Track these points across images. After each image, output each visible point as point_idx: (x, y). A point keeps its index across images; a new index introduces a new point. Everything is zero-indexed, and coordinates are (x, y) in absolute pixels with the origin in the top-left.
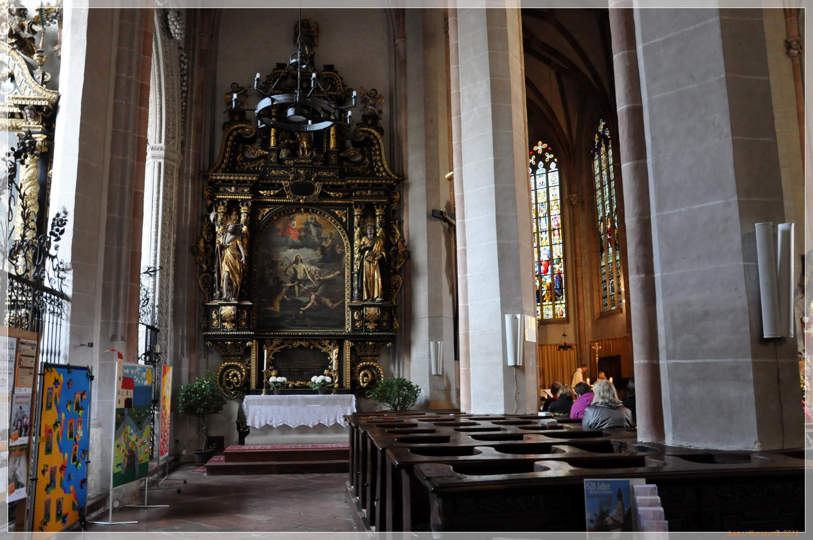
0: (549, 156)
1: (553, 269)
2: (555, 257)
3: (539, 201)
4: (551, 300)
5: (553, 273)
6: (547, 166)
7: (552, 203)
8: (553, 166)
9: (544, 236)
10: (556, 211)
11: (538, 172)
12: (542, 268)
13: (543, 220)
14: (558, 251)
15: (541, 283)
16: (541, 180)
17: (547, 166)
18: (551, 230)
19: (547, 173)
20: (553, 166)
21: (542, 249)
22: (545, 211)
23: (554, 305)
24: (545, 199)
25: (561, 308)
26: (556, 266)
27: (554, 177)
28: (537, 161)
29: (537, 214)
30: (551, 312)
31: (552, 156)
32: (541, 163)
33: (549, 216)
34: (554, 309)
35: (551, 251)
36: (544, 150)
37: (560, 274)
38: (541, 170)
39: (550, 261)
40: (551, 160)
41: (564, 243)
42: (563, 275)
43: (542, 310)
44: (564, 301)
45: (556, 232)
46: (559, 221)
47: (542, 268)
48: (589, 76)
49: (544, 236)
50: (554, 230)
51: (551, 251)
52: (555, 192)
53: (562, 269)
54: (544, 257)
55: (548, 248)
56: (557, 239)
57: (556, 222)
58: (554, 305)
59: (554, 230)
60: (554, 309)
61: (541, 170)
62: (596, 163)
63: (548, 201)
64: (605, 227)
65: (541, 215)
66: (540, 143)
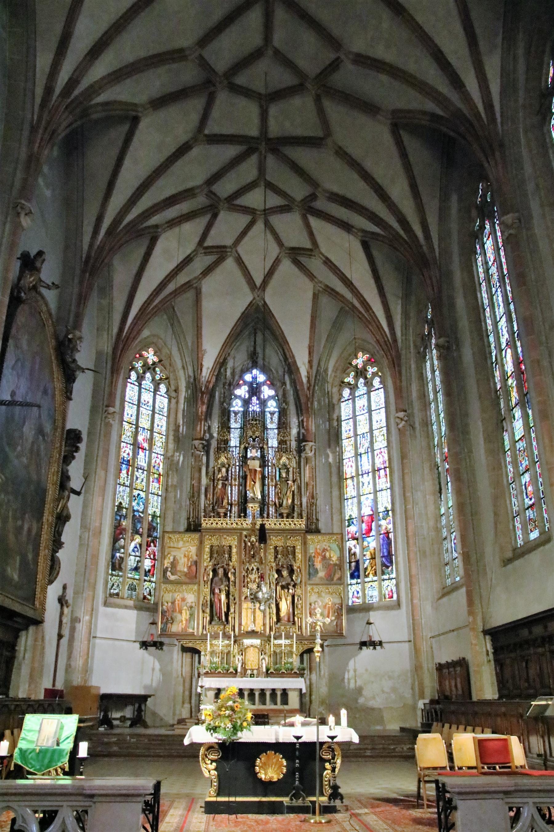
0: (371, 370)
2: (381, 509)
3: (359, 433)
4: (375, 574)
6: (369, 384)
8: (376, 382)
10: (381, 443)
13: (364, 457)
14: (385, 501)
15: (363, 549)
16: (361, 402)
17: (369, 384)
19: (369, 393)
20: (376, 382)
21: (363, 498)
22: (367, 445)
24: (367, 429)
25: (389, 586)
26: (383, 523)
28: (356, 377)
30: (376, 593)
31: (376, 369)
32: (362, 380)
33: (373, 451)
36: (365, 364)
37: (387, 533)
38: (362, 389)
40: (374, 374)
41: (391, 488)
42: (391, 536)
43: (364, 590)
44: (394, 575)
45: (382, 472)
46: (386, 457)
47: (364, 526)
48: (395, 225)
49: (367, 479)
50: (379, 470)
52: (380, 417)
53: (390, 526)
54: (367, 511)
55: (371, 496)
56: (383, 482)
57: (381, 459)
59: (379, 470)
61: (362, 389)
62: (428, 364)
63: (371, 430)
64: (442, 454)
66: (360, 354)
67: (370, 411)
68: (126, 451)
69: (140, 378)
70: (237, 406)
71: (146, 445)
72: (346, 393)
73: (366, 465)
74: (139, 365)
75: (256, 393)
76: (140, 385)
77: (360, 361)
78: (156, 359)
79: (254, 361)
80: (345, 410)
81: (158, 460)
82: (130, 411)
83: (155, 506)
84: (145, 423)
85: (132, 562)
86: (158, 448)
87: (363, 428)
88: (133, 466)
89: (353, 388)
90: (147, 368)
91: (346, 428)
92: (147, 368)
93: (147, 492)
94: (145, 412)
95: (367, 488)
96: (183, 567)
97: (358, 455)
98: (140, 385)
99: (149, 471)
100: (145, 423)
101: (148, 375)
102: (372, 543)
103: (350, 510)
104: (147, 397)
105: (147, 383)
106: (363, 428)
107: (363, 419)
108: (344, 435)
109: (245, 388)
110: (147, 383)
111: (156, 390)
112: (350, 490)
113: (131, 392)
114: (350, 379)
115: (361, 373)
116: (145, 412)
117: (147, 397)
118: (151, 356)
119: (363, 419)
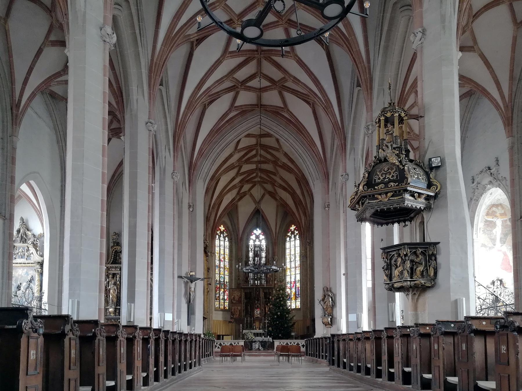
0: (296, 232)
1: (296, 285)
2: (297, 280)
5: (296, 288)
6: (295, 237)
7: (297, 255)
8: (297, 237)
9: (293, 270)
10: (298, 258)
11: (292, 240)
12: (292, 285)
14: (298, 277)
15: (291, 292)
16: (293, 243)
17: (295, 237)
18: (295, 267)
23: (296, 302)
26: (297, 284)
27: (298, 242)
29: (290, 259)
34: (296, 304)
35: (295, 277)
36: (295, 229)
38: (293, 239)
39: (295, 282)
47: (292, 285)
49: (293, 270)
51: (295, 277)
52: (298, 249)
54: (293, 280)
56: (298, 271)
57: (298, 263)
58: (296, 302)
60: (296, 304)
61: (293, 239)
65: (292, 260)
67: (295, 247)
68: (217, 263)
69: (220, 237)
70: (251, 243)
71: (223, 260)
72: (288, 239)
73: (293, 265)
74: (218, 232)
75: (257, 239)
76: (220, 240)
77: (293, 228)
78: (224, 229)
79: (257, 226)
80: (288, 245)
81: (227, 264)
82: (217, 249)
83: (227, 279)
84: (222, 252)
85: (221, 297)
86: (227, 260)
87: (293, 253)
88: (220, 267)
89: (290, 238)
90: (222, 233)
91: (288, 251)
92: (222, 233)
93: (224, 275)
94: (222, 248)
95: (293, 273)
96: (237, 298)
97: (291, 261)
98: (220, 240)
99: (224, 268)
100: (222, 252)
101: (222, 235)
102: (293, 290)
103: (288, 279)
104: (222, 243)
105: (222, 238)
106: (293, 253)
107: (293, 249)
108: (287, 254)
109: (254, 236)
110: (222, 238)
111: (225, 239)
112: (288, 273)
113: (217, 242)
114: (289, 234)
115: (293, 233)
116: (222, 248)
117: (222, 243)
118: (222, 228)
119: (293, 249)
